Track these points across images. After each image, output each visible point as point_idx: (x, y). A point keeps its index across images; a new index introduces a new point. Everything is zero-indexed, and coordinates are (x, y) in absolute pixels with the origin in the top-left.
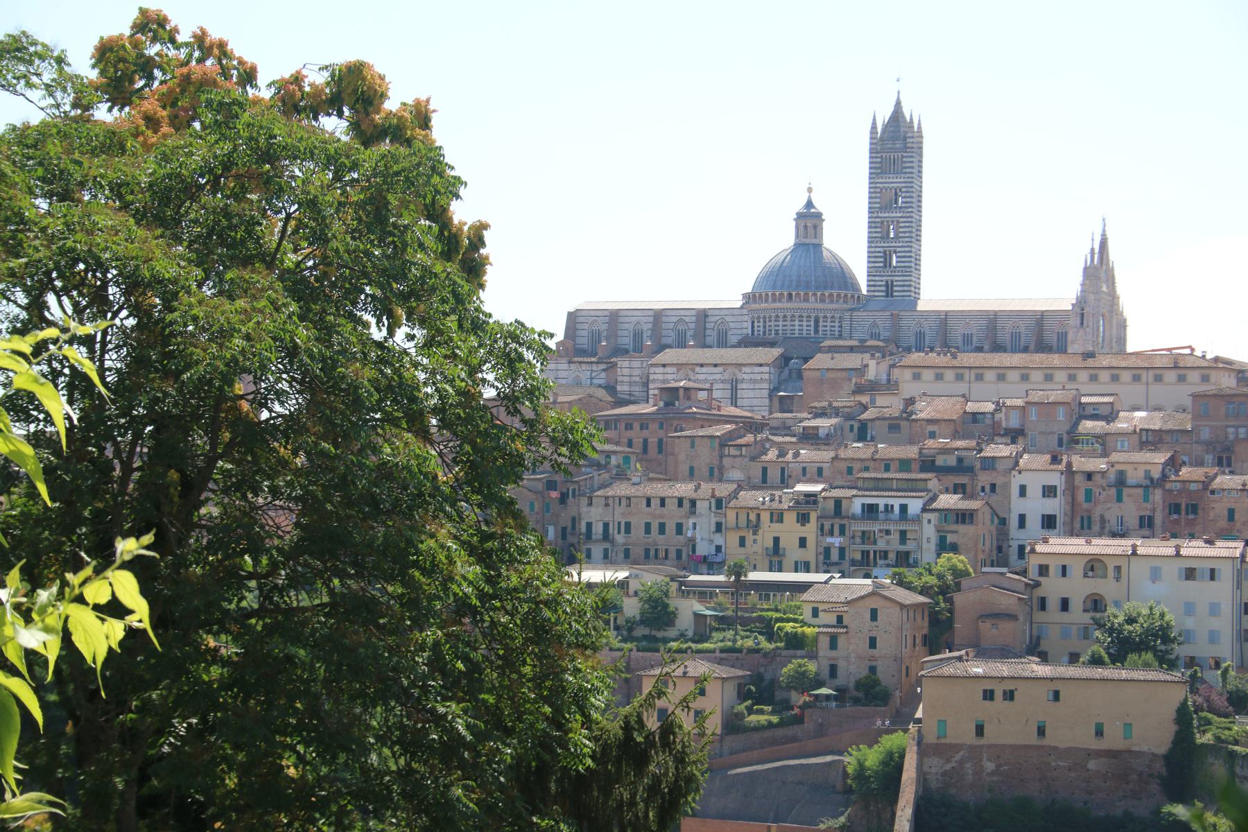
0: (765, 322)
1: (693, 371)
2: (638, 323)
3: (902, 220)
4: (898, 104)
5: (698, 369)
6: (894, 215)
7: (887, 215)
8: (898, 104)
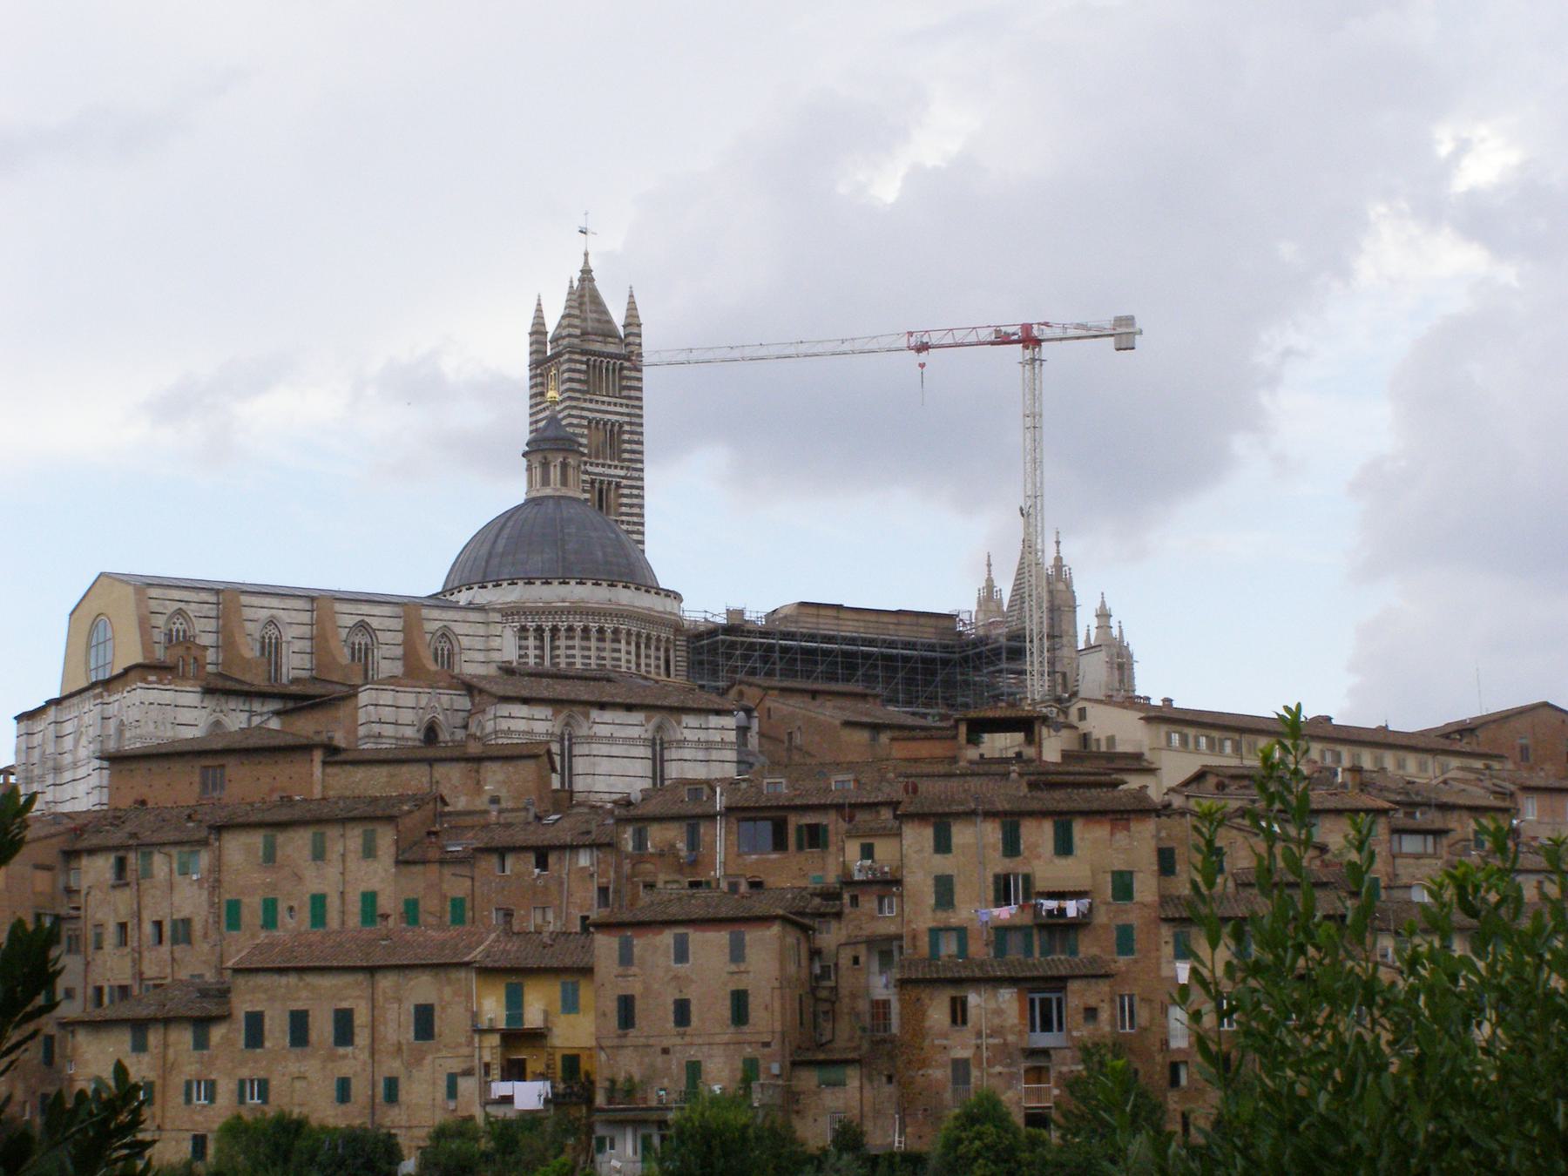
0: (553, 639)
1: (587, 716)
2: (271, 622)
3: (625, 482)
4: (586, 273)
5: (595, 714)
6: (612, 471)
7: (599, 470)
8: (586, 273)
